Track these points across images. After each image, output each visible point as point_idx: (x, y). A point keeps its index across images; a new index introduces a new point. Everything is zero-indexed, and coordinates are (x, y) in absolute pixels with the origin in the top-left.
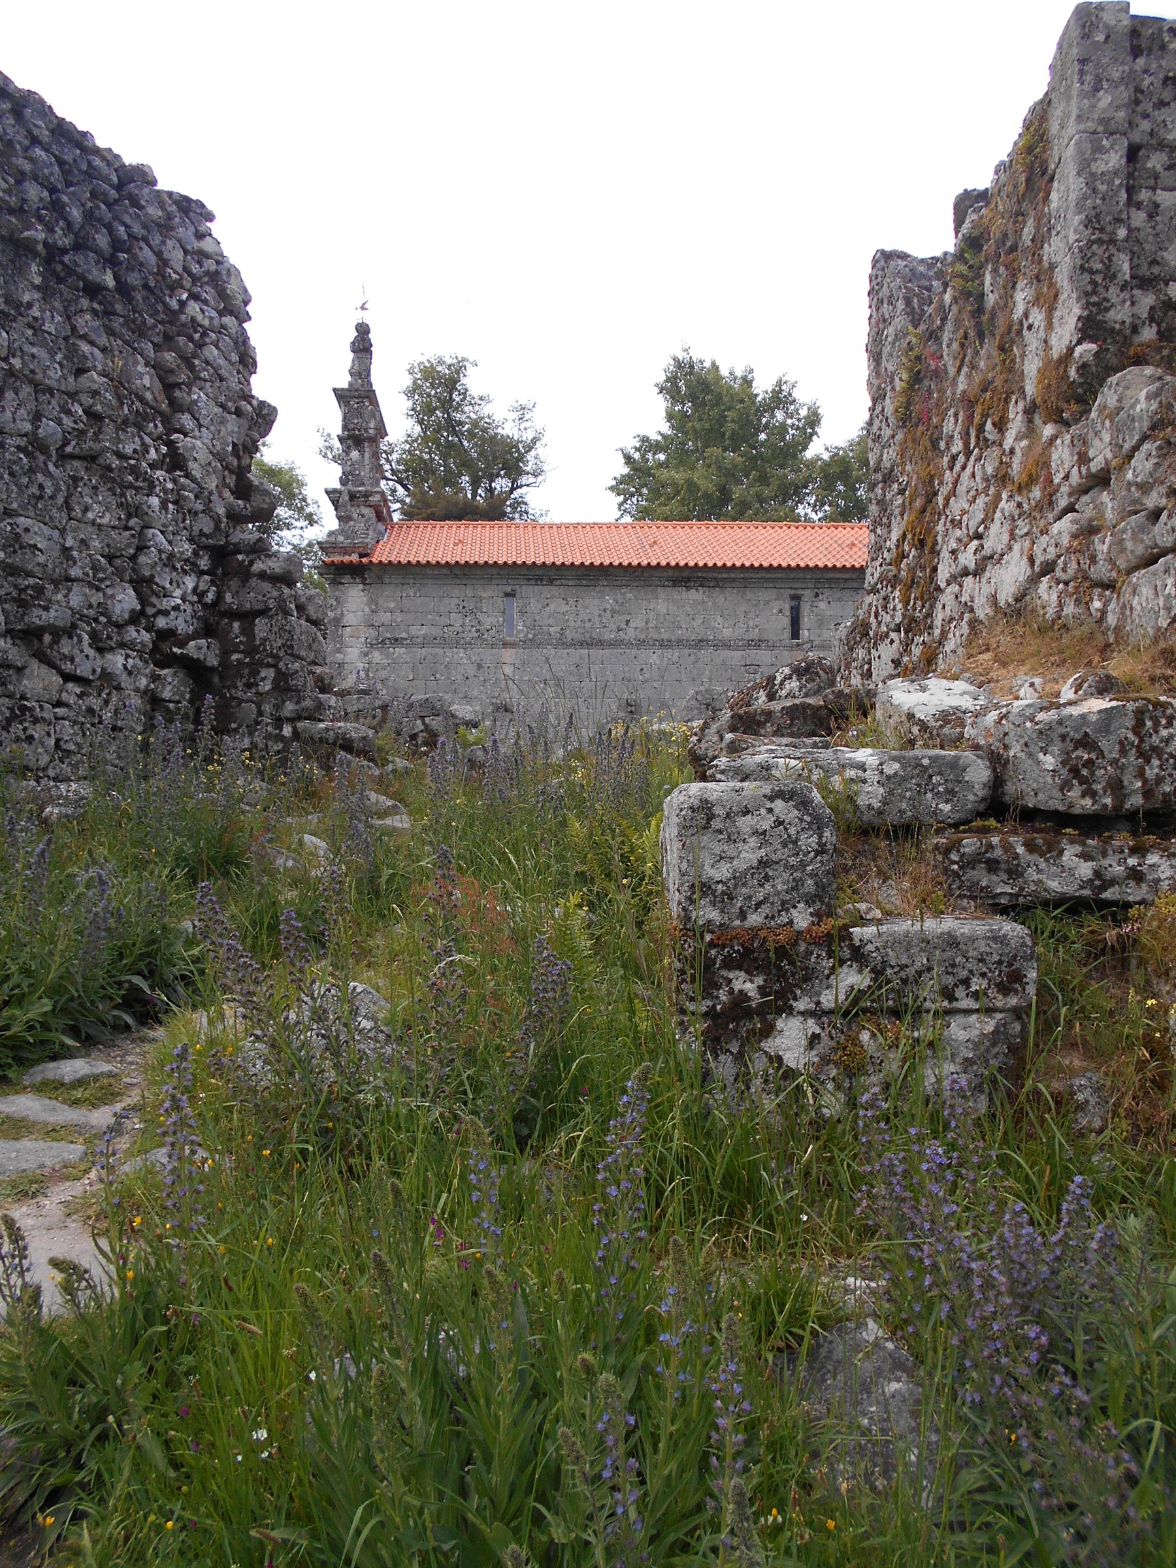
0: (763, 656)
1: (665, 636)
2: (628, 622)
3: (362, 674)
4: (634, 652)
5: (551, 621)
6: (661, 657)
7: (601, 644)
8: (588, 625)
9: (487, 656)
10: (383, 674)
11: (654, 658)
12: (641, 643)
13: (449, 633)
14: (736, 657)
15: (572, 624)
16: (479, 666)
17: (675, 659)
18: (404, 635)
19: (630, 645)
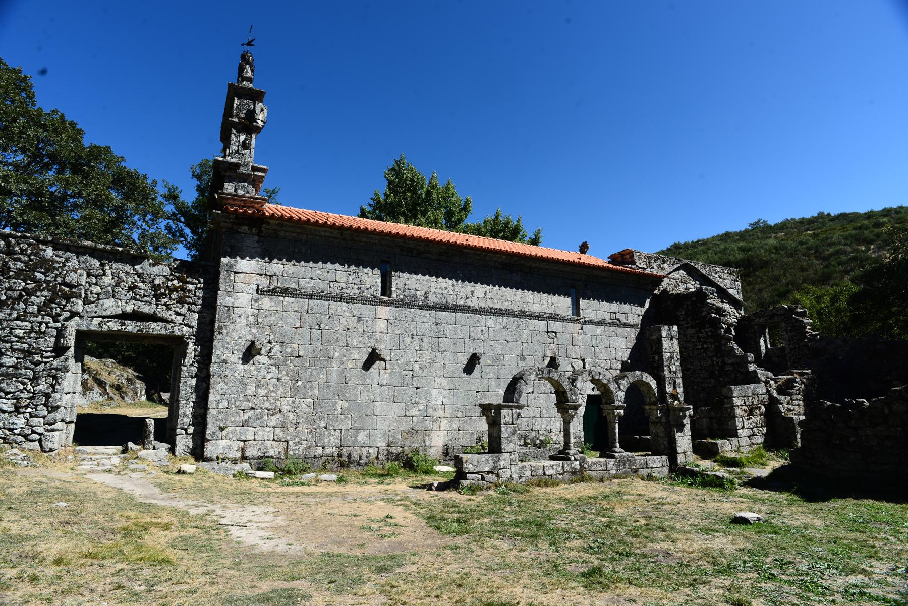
0: (555, 326)
1: (497, 306)
2: (473, 292)
3: (251, 319)
4: (477, 316)
5: (417, 286)
6: (496, 322)
7: (455, 308)
8: (445, 292)
9: (366, 310)
10: (272, 320)
11: (491, 321)
12: (482, 311)
13: (335, 290)
14: (541, 325)
15: (433, 290)
16: (359, 319)
17: (505, 324)
18: (294, 286)
19: (474, 311)
